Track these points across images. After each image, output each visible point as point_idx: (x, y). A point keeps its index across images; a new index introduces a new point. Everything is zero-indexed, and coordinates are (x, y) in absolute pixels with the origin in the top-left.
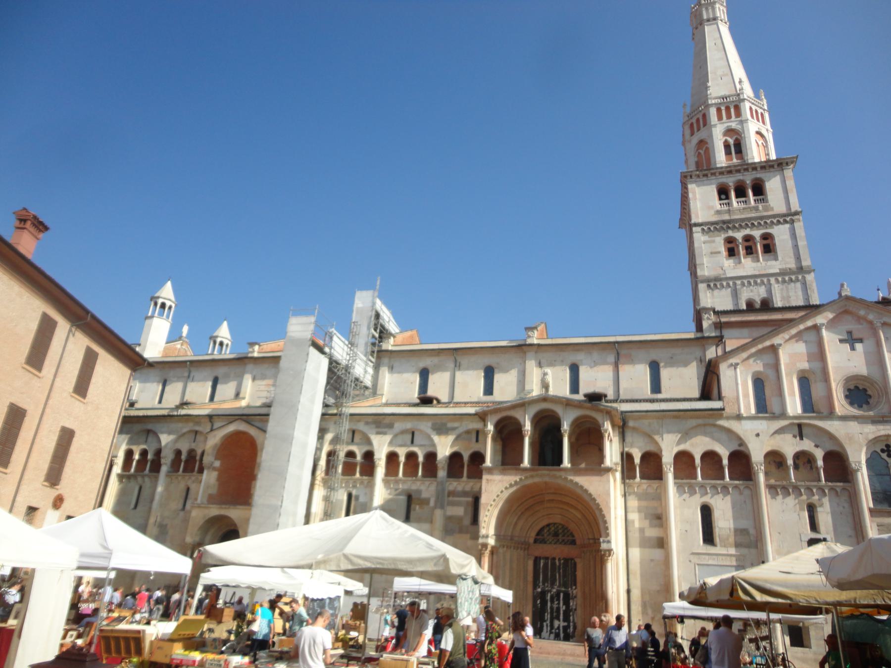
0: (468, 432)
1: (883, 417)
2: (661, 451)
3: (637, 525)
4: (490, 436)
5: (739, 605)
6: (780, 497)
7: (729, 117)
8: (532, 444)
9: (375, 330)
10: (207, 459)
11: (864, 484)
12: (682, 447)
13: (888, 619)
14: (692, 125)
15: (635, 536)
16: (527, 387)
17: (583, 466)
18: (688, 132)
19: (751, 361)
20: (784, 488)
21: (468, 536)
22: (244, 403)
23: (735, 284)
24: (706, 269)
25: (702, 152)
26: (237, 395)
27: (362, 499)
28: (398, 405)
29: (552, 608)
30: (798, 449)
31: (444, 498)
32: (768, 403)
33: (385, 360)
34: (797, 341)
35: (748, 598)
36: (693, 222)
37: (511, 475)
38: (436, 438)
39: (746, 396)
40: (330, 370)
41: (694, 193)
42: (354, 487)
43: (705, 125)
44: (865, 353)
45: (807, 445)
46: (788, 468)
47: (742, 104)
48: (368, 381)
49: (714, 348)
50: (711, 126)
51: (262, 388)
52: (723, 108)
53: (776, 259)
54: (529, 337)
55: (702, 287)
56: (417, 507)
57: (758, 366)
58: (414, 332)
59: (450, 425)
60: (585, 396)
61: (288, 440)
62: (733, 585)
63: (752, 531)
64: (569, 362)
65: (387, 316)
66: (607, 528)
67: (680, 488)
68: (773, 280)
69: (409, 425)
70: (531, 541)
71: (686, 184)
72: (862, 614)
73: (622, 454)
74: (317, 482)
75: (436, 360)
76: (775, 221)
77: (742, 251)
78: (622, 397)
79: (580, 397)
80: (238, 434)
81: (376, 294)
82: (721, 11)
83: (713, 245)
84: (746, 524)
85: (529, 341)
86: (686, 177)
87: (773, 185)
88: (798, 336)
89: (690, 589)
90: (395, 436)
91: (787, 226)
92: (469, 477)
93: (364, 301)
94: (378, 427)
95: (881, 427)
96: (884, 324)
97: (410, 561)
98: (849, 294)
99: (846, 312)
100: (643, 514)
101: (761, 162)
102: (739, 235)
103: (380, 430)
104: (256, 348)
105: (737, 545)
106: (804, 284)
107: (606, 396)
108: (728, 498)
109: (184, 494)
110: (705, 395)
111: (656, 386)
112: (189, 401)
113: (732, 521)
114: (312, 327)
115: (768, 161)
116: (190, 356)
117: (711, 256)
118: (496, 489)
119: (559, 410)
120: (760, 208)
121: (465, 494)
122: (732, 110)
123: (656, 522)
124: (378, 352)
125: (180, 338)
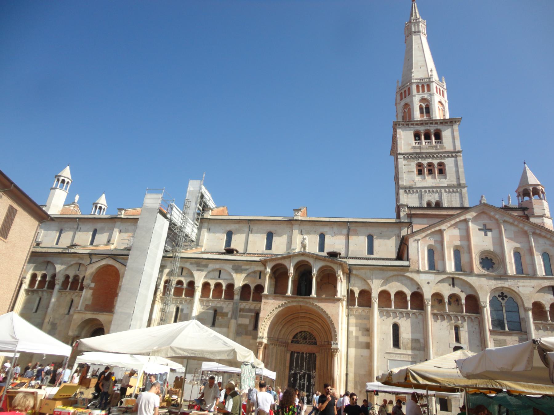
0: (255, 272)
1: (500, 276)
2: (371, 290)
3: (354, 334)
4: (268, 275)
5: (409, 386)
6: (439, 321)
7: (423, 91)
8: (293, 281)
9: (200, 205)
10: (86, 282)
11: (487, 315)
12: (384, 288)
13: (495, 396)
14: (401, 94)
15: (353, 341)
16: (293, 246)
17: (324, 296)
18: (399, 98)
19: (427, 238)
20: (442, 315)
21: (251, 337)
22: (113, 247)
23: (421, 191)
24: (405, 181)
25: (406, 111)
26: (109, 242)
27: (185, 312)
28: (212, 253)
29: (300, 384)
30: (451, 292)
31: (237, 312)
32: (436, 264)
33: (206, 225)
34: (454, 228)
35: (415, 382)
36: (398, 152)
37: (279, 300)
38: (234, 275)
39: (423, 259)
40: (170, 229)
41: (400, 135)
42: (181, 303)
43: (409, 95)
44: (493, 238)
45: (456, 290)
46: (445, 303)
47: (431, 84)
48: (194, 237)
49: (406, 229)
50: (413, 96)
51: (126, 238)
52: (420, 85)
53: (446, 178)
54: (296, 215)
55: (401, 191)
57: (431, 241)
58: (225, 208)
59: (243, 267)
60: (328, 253)
61: (140, 272)
62: (407, 373)
63: (422, 341)
64: (319, 233)
65: (208, 198)
66: (336, 336)
67: (381, 312)
68: (443, 190)
69: (218, 266)
70: (290, 341)
71: (396, 129)
72: (481, 393)
73: (348, 291)
74: (157, 299)
75: (237, 226)
76: (446, 155)
77: (426, 172)
78: (350, 255)
79: (324, 254)
80: (107, 266)
81: (202, 182)
82: (423, 27)
83: (410, 167)
84: (419, 336)
85: (296, 218)
86: (396, 125)
87: (446, 134)
88: (455, 225)
89: (383, 374)
90: (209, 272)
91: (453, 159)
92: (253, 300)
93: (194, 187)
94: (197, 266)
95: (499, 282)
96: (504, 221)
97: (212, 353)
98: (485, 202)
99: (483, 213)
100: (358, 328)
101: (440, 120)
102: (425, 162)
103: (199, 268)
104: (123, 212)
105: (413, 349)
106: (461, 194)
107: (340, 254)
108: (409, 320)
109: (70, 304)
110: (400, 257)
111: (371, 250)
112: (77, 244)
113: (410, 334)
114: (160, 201)
115: (444, 119)
116: (79, 214)
117: (408, 174)
118: (270, 308)
119: (311, 261)
121: (250, 310)
122: (426, 87)
123: (366, 333)
124: (201, 219)
125: (73, 203)
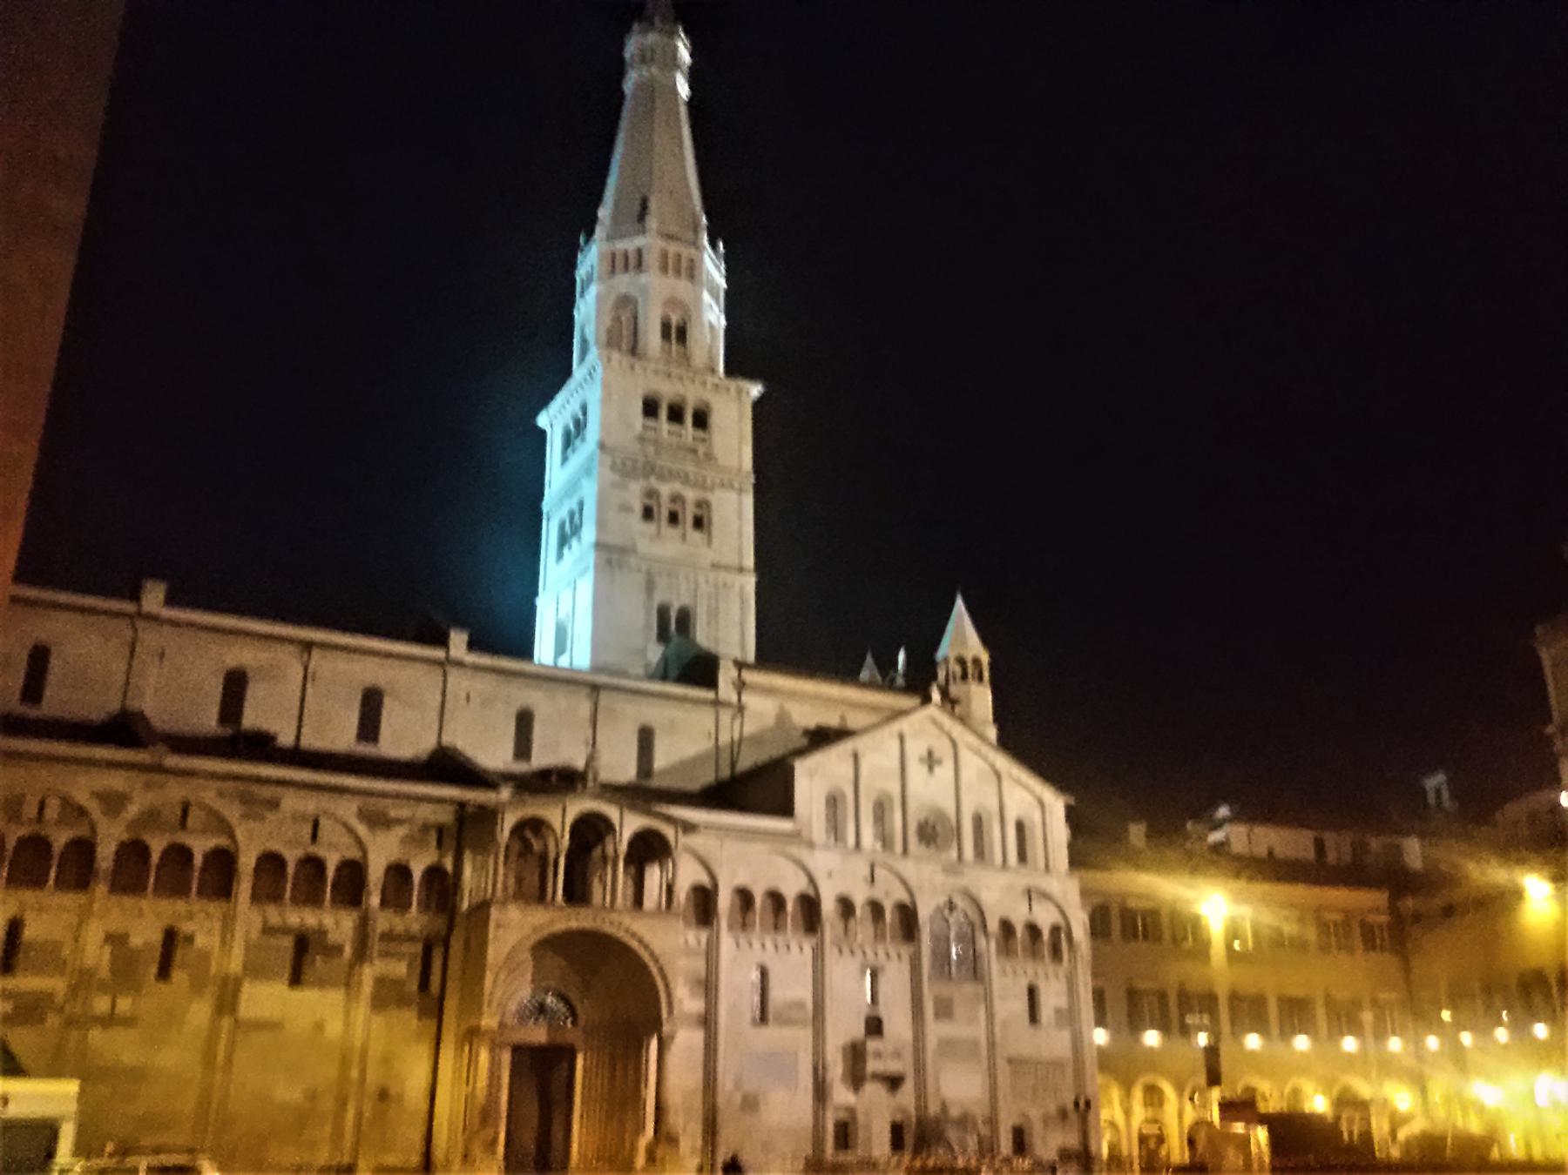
0: (425, 828)
2: (716, 886)
59: (393, 813)
91: (733, 496)
119: (612, 812)
121: (409, 938)
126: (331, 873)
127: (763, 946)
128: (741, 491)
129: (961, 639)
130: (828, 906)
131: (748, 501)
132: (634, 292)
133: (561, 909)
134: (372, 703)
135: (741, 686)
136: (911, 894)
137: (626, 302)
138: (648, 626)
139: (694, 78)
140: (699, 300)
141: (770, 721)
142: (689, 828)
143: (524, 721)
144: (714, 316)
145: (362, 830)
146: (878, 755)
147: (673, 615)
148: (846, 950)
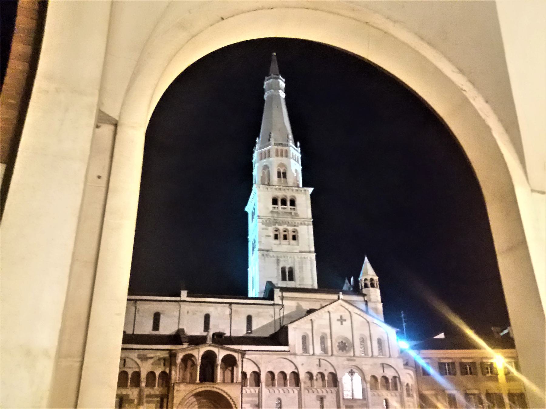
0: (159, 359)
2: (260, 371)
30: (318, 371)
53: (298, 245)
56: (126, 405)
59: (149, 355)
91: (306, 227)
102: (281, 228)
119: (215, 350)
120: (293, 214)
121: (156, 396)
126: (130, 376)
127: (279, 391)
128: (308, 225)
129: (366, 273)
130: (303, 376)
131: (311, 227)
132: (267, 164)
133: (198, 384)
134: (157, 317)
135: (282, 298)
136: (335, 370)
137: (266, 167)
138: (279, 275)
139: (286, 91)
140: (290, 163)
141: (294, 309)
142: (243, 353)
143: (207, 318)
144: (295, 168)
145: (138, 361)
146: (320, 319)
147: (287, 270)
148: (310, 391)
